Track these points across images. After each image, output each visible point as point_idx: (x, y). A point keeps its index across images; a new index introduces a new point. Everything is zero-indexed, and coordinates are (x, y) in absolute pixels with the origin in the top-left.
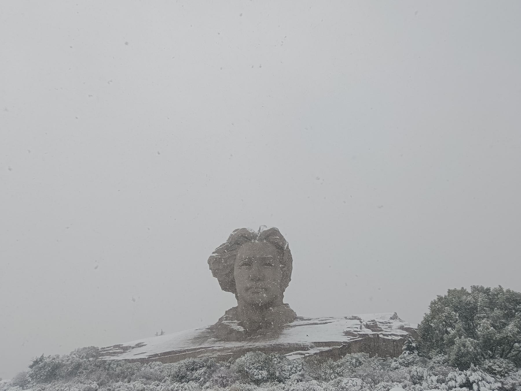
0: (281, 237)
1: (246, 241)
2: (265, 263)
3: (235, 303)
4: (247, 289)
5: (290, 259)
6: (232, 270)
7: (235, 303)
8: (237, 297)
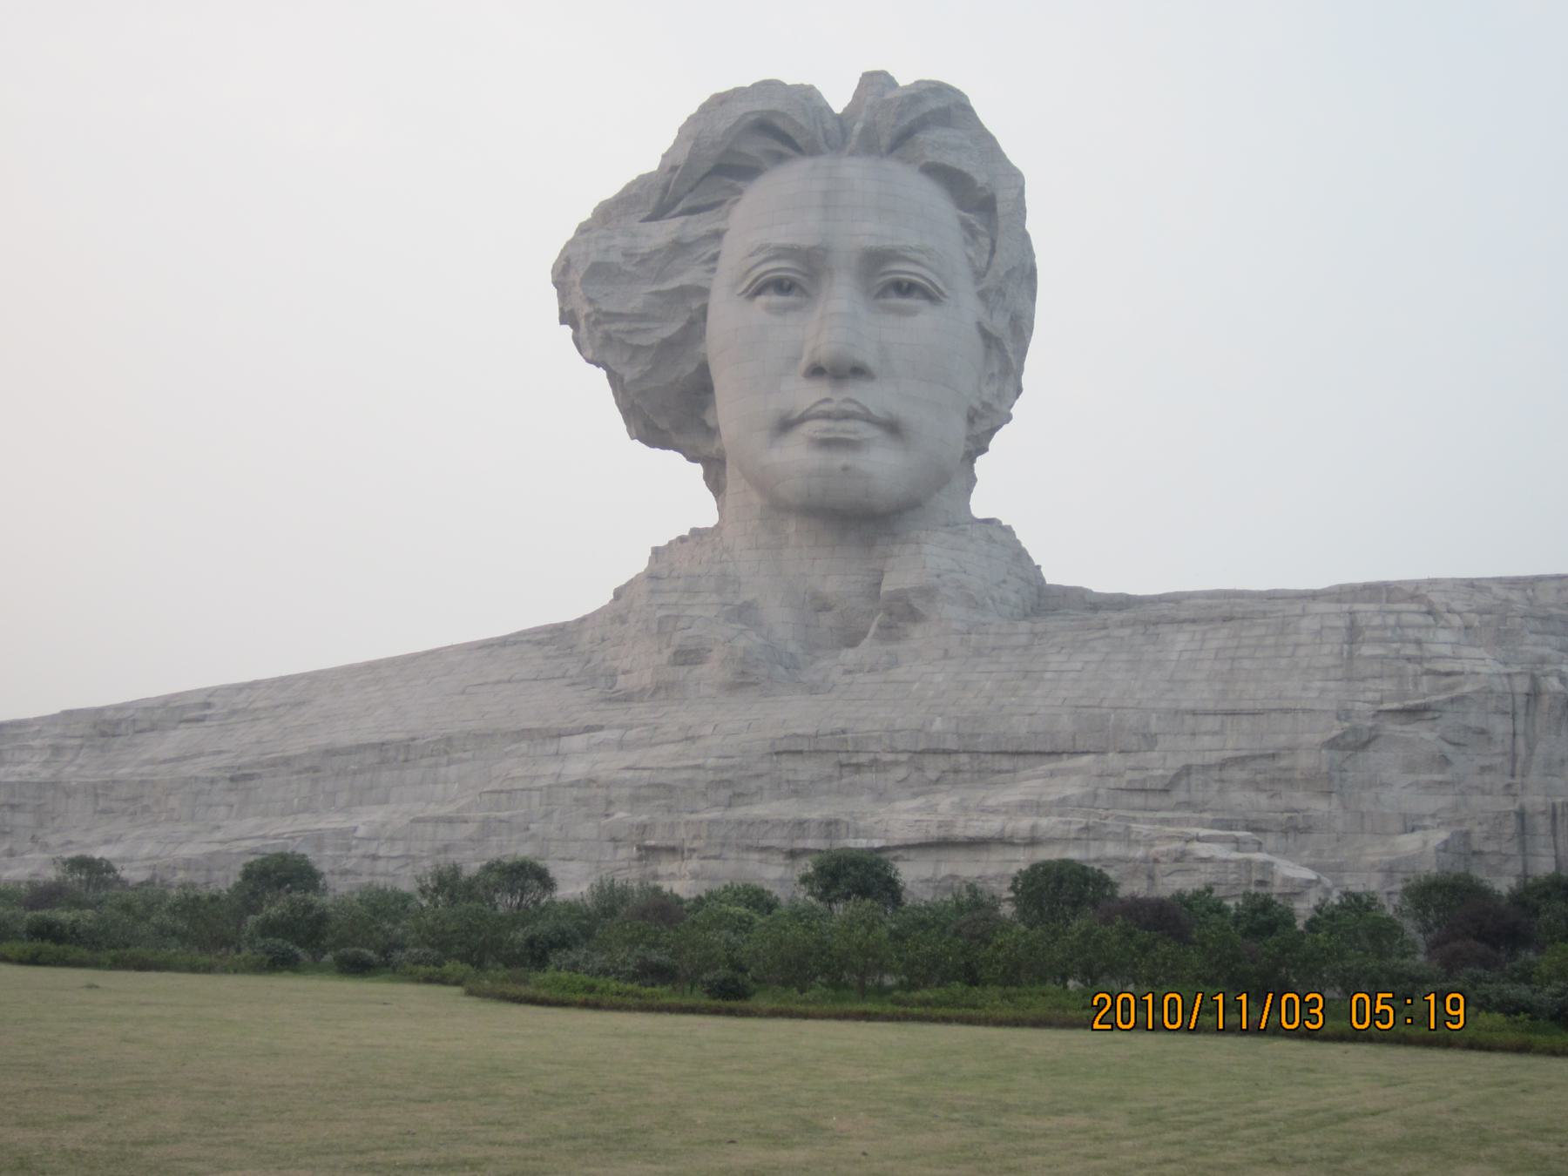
0: (987, 145)
1: (780, 158)
2: (893, 283)
3: (703, 510)
4: (786, 425)
5: (1028, 276)
6: (697, 323)
7: (703, 510)
8: (715, 482)
